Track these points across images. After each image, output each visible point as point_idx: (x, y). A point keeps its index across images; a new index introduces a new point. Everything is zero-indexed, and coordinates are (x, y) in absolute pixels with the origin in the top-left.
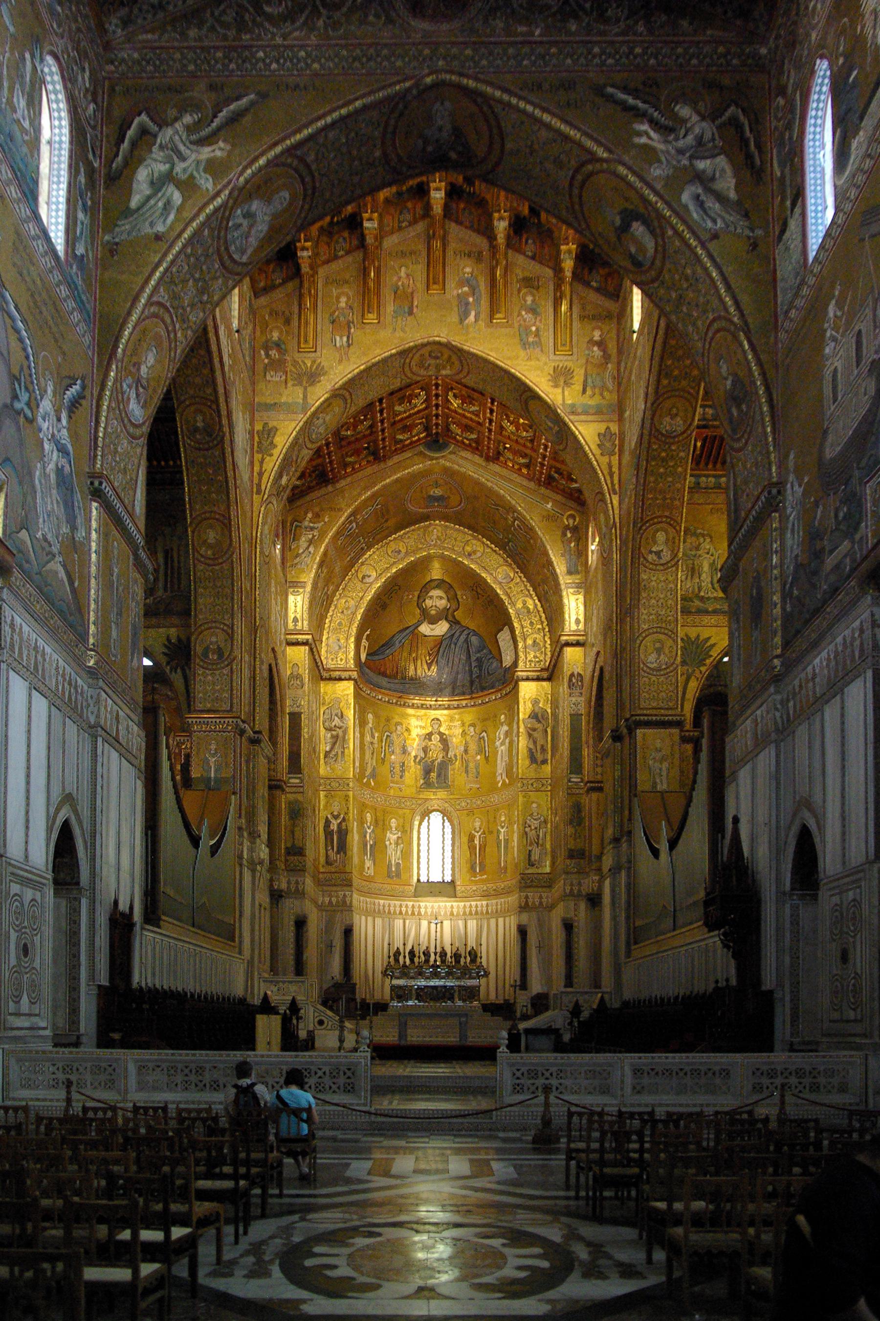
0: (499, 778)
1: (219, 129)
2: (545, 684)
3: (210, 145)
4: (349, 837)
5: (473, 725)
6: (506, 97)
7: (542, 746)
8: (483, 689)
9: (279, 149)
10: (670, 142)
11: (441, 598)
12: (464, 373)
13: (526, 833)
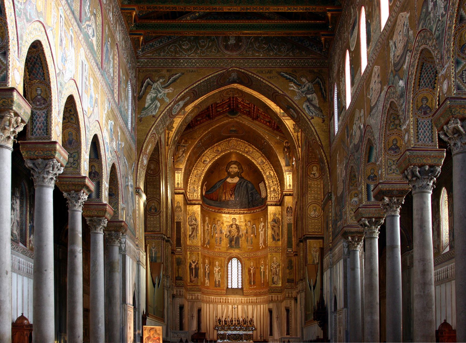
0: (260, 245)
1: (170, 84)
2: (278, 207)
3: (168, 89)
4: (199, 271)
5: (249, 221)
6: (253, 75)
7: (278, 233)
8: (253, 206)
9: (187, 90)
10: (299, 89)
11: (236, 168)
12: (244, 96)
13: (271, 270)
